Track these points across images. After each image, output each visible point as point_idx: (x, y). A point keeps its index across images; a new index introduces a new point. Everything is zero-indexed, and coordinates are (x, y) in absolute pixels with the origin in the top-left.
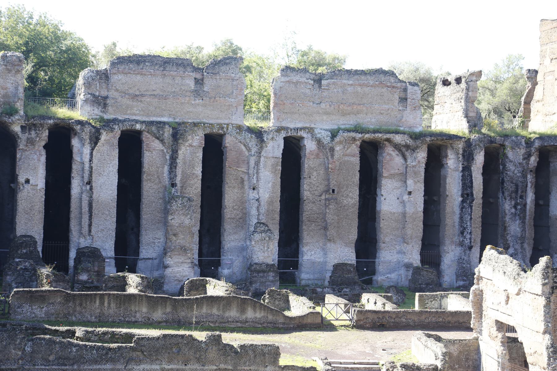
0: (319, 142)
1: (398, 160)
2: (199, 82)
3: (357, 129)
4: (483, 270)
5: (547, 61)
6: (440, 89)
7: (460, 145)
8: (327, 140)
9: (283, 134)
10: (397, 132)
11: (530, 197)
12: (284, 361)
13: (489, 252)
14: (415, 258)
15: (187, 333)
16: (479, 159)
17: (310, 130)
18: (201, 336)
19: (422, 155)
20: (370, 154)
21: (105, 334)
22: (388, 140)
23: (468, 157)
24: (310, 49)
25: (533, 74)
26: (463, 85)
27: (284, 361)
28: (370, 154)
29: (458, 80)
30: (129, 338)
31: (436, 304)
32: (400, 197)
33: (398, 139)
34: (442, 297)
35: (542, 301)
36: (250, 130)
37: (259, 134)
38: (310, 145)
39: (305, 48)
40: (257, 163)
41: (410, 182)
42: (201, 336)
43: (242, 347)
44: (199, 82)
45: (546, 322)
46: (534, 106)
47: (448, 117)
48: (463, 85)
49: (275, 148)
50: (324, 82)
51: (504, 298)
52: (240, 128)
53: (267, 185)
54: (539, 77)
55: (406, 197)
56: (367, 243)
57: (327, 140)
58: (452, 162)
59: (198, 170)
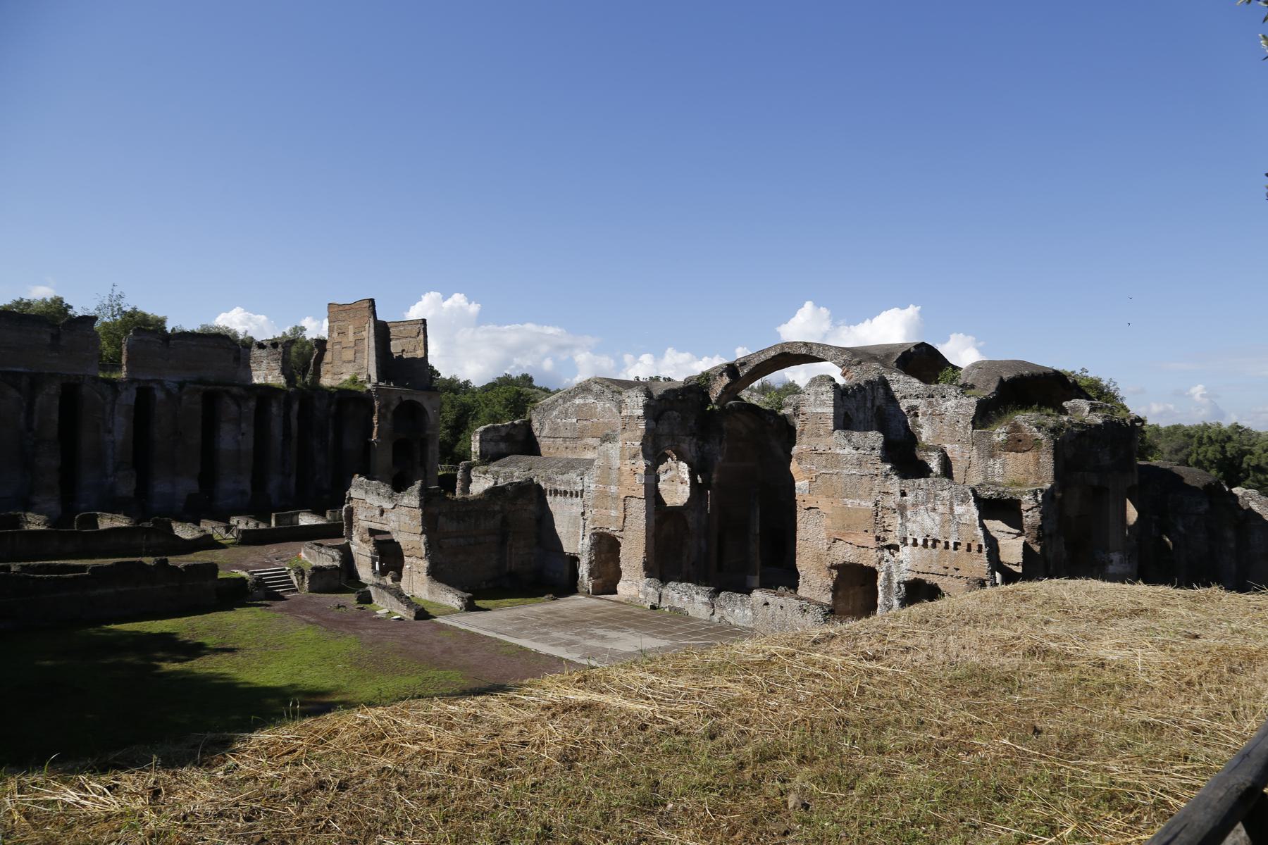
0: (168, 392)
1: (234, 408)
2: (56, 337)
3: (201, 381)
4: (353, 492)
5: (335, 335)
6: (256, 352)
7: (282, 397)
8: (175, 390)
9: (136, 385)
10: (235, 385)
11: (331, 436)
12: (222, 575)
13: (357, 479)
14: (246, 485)
15: (138, 559)
16: (296, 407)
17: (160, 382)
18: (149, 561)
19: (252, 404)
20: (211, 400)
21: (40, 566)
22: (227, 392)
23: (287, 405)
24: (135, 309)
25: (321, 344)
26: (280, 349)
27: (222, 575)
28: (211, 400)
29: (274, 344)
30: (83, 568)
31: (287, 521)
32: (233, 438)
33: (235, 390)
34: (293, 515)
35: (419, 512)
36: (105, 381)
37: (113, 384)
38: (160, 395)
39: (128, 309)
40: (113, 410)
41: (243, 425)
42: (149, 561)
43: (186, 567)
44: (56, 337)
45: (423, 525)
46: (324, 368)
47: (266, 374)
48: (280, 349)
49: (128, 397)
50: (172, 342)
51: (378, 512)
52: (96, 379)
53: (120, 428)
54: (328, 346)
55: (240, 437)
56: (208, 477)
57: (175, 390)
58: (275, 409)
59: (55, 416)
